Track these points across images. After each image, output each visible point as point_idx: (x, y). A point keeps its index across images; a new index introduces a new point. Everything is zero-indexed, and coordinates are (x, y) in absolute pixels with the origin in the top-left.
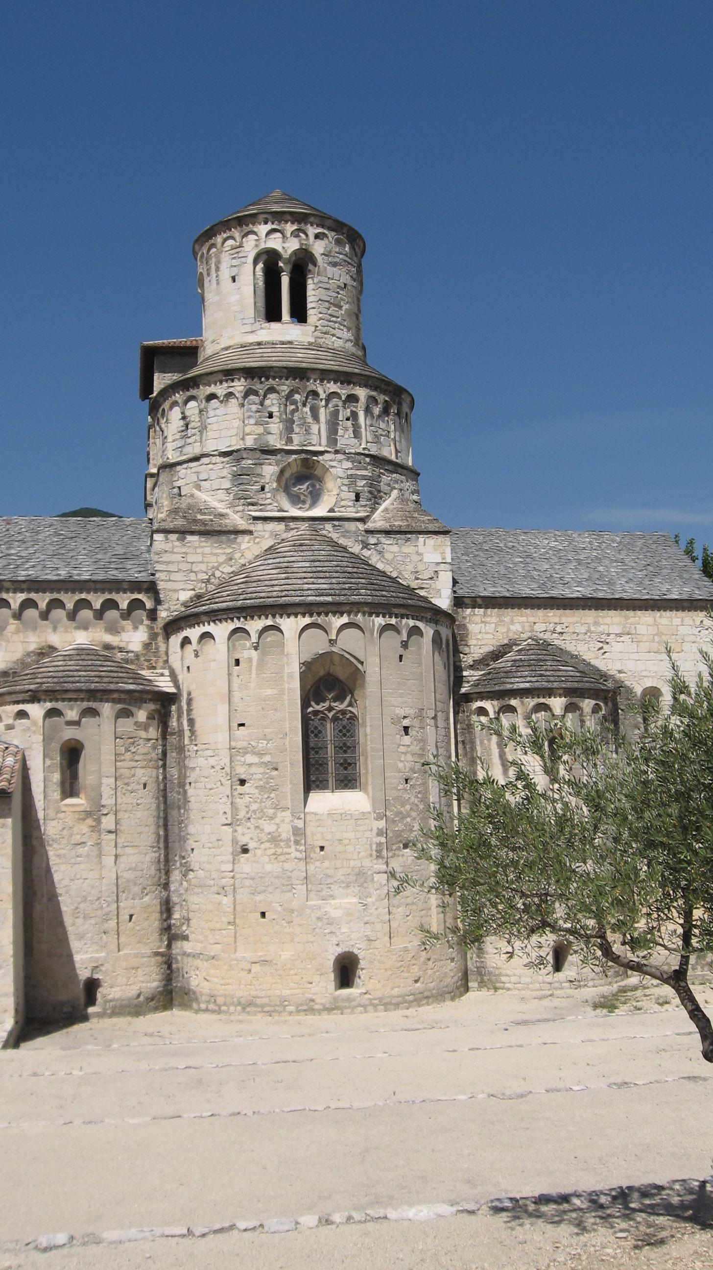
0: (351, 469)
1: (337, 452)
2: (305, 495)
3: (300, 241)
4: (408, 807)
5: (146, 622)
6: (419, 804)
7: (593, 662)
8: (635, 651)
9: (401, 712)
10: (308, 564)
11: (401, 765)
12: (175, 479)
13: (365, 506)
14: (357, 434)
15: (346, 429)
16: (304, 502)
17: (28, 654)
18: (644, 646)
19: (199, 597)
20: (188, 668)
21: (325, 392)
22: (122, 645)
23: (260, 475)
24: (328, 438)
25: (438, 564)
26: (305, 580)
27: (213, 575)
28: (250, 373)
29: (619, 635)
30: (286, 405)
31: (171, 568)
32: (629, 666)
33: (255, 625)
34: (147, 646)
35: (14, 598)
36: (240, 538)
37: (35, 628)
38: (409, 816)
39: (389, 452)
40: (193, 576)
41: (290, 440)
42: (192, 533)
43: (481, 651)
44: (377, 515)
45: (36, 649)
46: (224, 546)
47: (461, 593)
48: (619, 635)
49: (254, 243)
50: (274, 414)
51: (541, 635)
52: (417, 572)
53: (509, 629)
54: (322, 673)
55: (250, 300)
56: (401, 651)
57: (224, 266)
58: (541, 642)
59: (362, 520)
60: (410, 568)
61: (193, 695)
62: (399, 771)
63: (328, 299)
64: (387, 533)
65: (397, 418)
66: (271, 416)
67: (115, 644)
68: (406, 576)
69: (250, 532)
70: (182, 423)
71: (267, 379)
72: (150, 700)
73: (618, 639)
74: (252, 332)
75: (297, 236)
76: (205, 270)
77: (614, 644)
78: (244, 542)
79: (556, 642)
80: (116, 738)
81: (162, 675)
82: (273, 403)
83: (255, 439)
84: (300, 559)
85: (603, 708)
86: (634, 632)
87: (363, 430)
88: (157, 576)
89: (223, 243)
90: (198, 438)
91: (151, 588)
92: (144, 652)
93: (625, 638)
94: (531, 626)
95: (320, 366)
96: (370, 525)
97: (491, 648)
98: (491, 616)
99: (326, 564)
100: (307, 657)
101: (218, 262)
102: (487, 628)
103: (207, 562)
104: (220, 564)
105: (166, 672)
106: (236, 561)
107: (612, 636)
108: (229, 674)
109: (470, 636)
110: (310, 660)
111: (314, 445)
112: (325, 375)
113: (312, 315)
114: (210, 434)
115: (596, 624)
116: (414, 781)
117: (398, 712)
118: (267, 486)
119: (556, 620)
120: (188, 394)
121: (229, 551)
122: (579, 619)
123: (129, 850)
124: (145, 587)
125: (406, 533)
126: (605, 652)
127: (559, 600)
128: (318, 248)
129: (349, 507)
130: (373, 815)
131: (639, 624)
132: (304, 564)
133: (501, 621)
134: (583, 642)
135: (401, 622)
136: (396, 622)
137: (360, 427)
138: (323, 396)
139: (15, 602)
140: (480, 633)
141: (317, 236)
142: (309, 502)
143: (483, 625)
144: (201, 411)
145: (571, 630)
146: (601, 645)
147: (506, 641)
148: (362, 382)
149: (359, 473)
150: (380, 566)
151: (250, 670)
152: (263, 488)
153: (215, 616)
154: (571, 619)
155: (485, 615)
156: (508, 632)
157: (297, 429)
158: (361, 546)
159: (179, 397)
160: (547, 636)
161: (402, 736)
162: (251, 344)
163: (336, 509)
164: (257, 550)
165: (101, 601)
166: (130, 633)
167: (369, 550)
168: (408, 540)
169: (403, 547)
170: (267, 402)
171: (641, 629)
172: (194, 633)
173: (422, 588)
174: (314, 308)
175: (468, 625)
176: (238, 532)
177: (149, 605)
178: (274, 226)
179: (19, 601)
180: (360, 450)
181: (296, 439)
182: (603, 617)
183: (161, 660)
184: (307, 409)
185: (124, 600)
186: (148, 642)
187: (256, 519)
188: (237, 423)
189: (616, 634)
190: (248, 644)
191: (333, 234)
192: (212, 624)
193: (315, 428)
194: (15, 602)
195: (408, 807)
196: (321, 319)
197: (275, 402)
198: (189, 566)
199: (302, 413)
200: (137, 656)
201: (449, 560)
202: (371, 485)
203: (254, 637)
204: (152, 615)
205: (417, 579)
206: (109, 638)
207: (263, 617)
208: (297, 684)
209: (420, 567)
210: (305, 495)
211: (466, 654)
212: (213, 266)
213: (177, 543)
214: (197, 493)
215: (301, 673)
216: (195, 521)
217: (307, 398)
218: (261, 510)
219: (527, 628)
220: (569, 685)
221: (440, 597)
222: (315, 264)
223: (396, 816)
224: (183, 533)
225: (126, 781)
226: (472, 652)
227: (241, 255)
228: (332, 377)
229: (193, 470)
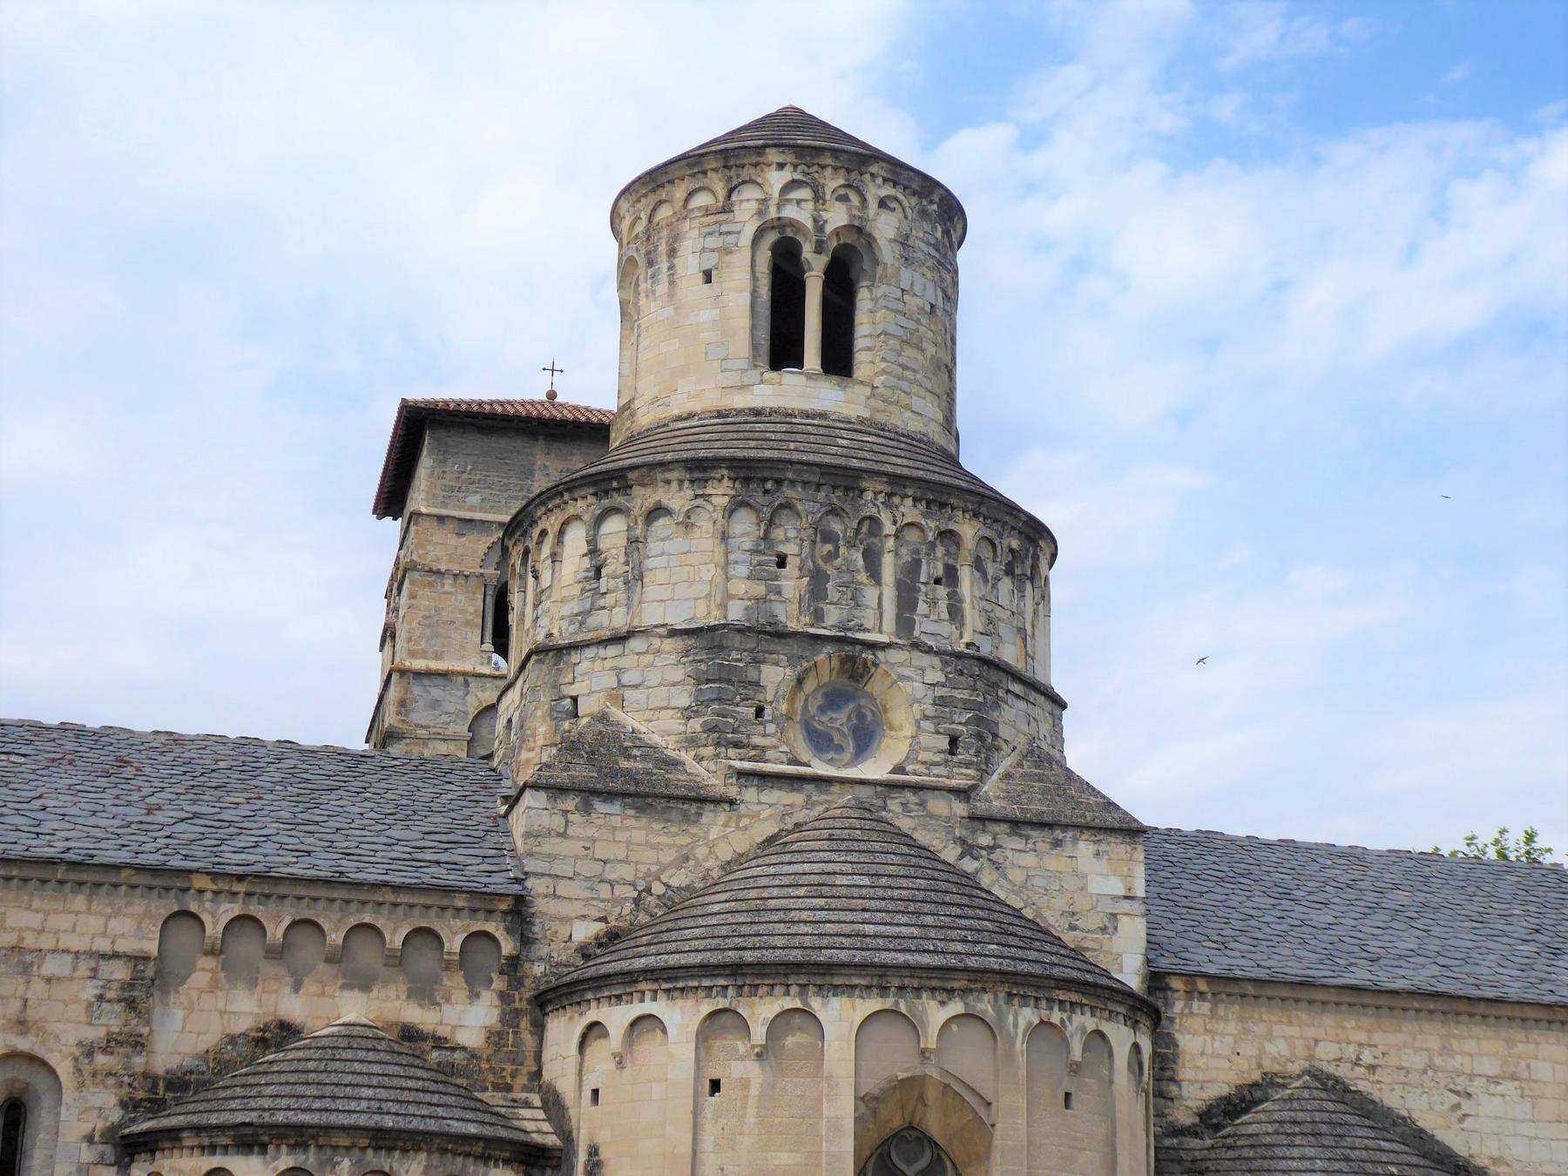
0: (943, 685)
1: (916, 645)
2: (843, 734)
3: (849, 209)
5: (499, 983)
7: (1440, 1135)
10: (866, 881)
12: (566, 680)
13: (968, 765)
14: (955, 613)
15: (933, 603)
16: (840, 749)
17: (233, 1040)
19: (613, 936)
20: (596, 1092)
21: (895, 523)
22: (443, 1031)
23: (756, 684)
24: (899, 618)
25: (1115, 898)
26: (867, 915)
27: (648, 890)
28: (747, 472)
29: (1495, 1080)
30: (814, 542)
31: (557, 869)
33: (762, 1011)
34: (496, 1038)
35: (213, 915)
36: (708, 815)
37: (252, 983)
39: (1009, 654)
40: (604, 890)
41: (818, 616)
42: (610, 796)
43: (1205, 1096)
44: (991, 786)
45: (251, 1030)
46: (674, 829)
47: (1164, 963)
48: (1495, 1080)
49: (754, 206)
50: (789, 559)
51: (1331, 1069)
52: (1073, 914)
53: (1262, 1050)
54: (897, 1122)
55: (742, 322)
56: (1068, 1084)
57: (688, 246)
58: (1330, 1083)
59: (963, 794)
60: (1060, 903)
61: (604, 1154)
63: (900, 332)
64: (1016, 825)
66: (781, 562)
67: (427, 1028)
69: (732, 802)
70: (586, 562)
71: (779, 482)
72: (506, 1162)
73: (1493, 1088)
74: (743, 387)
75: (844, 199)
76: (643, 251)
77: (1483, 1098)
78: (714, 823)
79: (1363, 1086)
81: (527, 1105)
82: (790, 538)
83: (747, 609)
84: (848, 868)
86: (1525, 1075)
88: (529, 884)
89: (687, 200)
90: (622, 596)
91: (519, 912)
92: (490, 1051)
93: (1508, 1087)
94: (1308, 1048)
95: (889, 469)
96: (981, 807)
97: (1224, 1090)
98: (1226, 1019)
99: (904, 883)
100: (871, 1085)
101: (676, 238)
102: (1217, 1044)
103: (637, 863)
104: (664, 868)
105: (536, 1099)
106: (698, 863)
107: (1478, 1082)
108: (696, 1113)
109: (1180, 1061)
110: (876, 1092)
111: (868, 630)
112: (898, 482)
113: (865, 361)
114: (651, 592)
115: (1446, 1051)
118: (768, 711)
119: (1362, 1037)
120: (606, 502)
121: (683, 840)
124: (503, 906)
125: (1049, 826)
126: (1465, 1115)
128: (885, 227)
131: (1536, 1058)
132: (857, 880)
133: (1247, 1032)
134: (1419, 1091)
135: (1070, 1019)
136: (1062, 1021)
137: (961, 601)
139: (215, 923)
140: (1202, 1054)
141: (882, 204)
142: (850, 747)
143: (1209, 1039)
144: (633, 541)
145: (1392, 1060)
146: (1455, 1099)
147: (1256, 1076)
149: (957, 694)
151: (744, 1107)
152: (759, 712)
153: (670, 979)
154: (1393, 1038)
155: (1213, 1015)
158: (960, 850)
159: (585, 506)
160: (1343, 1071)
162: (739, 412)
163: (909, 768)
164: (741, 843)
165: (405, 931)
166: (459, 1008)
167: (976, 859)
168: (1057, 844)
169: (1046, 858)
170: (778, 534)
171: (1542, 1071)
172: (617, 1017)
174: (869, 349)
175: (1177, 1036)
176: (702, 800)
177: (508, 946)
178: (798, 176)
179: (224, 920)
180: (961, 648)
181: (833, 615)
182: (1460, 1038)
183: (524, 1070)
185: (455, 933)
186: (499, 1027)
187: (741, 774)
188: (709, 572)
189: (1488, 1077)
190: (742, 1047)
191: (914, 200)
192: (661, 996)
193: (870, 594)
194: (215, 923)
196: (884, 372)
197: (792, 534)
198: (598, 867)
199: (848, 561)
200: (473, 1055)
201: (1140, 892)
202: (978, 721)
203: (759, 1034)
204: (513, 966)
205: (1073, 928)
206: (415, 1015)
207: (778, 990)
208: (847, 1145)
209: (1081, 904)
210: (843, 734)
211: (1172, 1099)
212: (663, 248)
214: (616, 713)
215: (856, 1119)
216: (616, 773)
217: (857, 531)
218: (750, 759)
219: (1301, 1051)
222: (876, 262)
224: (589, 794)
226: (1185, 1094)
227: (724, 228)
228: (910, 492)
229: (608, 664)
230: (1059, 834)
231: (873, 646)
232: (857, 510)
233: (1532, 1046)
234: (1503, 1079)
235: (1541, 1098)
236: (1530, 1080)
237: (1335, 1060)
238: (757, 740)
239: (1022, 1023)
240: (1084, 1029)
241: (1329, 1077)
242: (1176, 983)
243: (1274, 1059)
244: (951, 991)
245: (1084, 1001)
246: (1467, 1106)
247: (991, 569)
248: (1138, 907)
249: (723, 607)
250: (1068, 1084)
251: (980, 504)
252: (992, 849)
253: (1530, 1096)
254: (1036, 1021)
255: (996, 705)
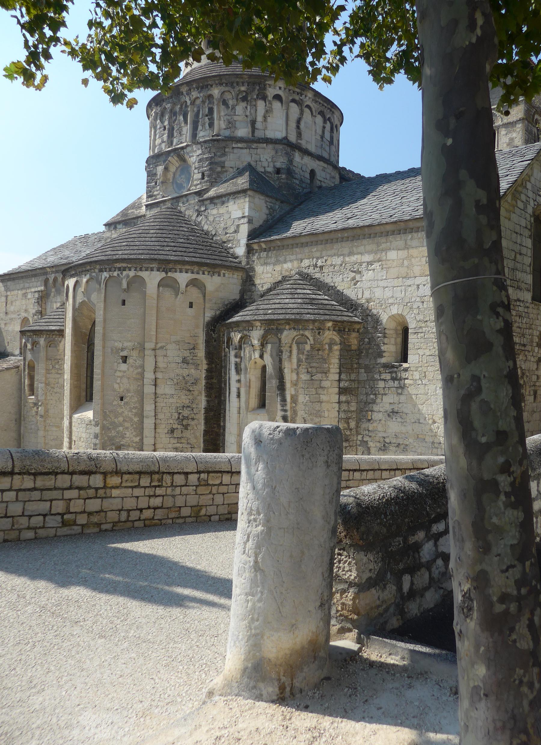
4: (121, 419)
6: (133, 417)
8: (384, 277)
9: (119, 345)
11: (116, 386)
14: (211, 125)
15: (203, 125)
18: (394, 272)
23: (156, 174)
25: (240, 219)
29: (370, 263)
32: (378, 293)
38: (121, 425)
39: (243, 132)
41: (171, 143)
48: (370, 263)
51: (306, 271)
53: (282, 268)
60: (222, 225)
62: (114, 390)
65: (261, 104)
68: (220, 233)
77: (364, 273)
79: (317, 276)
80: (47, 359)
85: (311, 338)
87: (216, 122)
98: (271, 257)
107: (364, 265)
109: (256, 277)
115: (351, 254)
116: (128, 398)
117: (116, 344)
118: (158, 181)
119: (318, 254)
122: (336, 251)
123: (54, 429)
126: (358, 281)
127: (320, 236)
129: (198, 185)
130: (93, 423)
134: (339, 273)
135: (122, 273)
136: (118, 274)
138: (189, 102)
147: (280, 278)
148: (217, 82)
150: (206, 228)
155: (267, 256)
156: (281, 271)
157: (175, 134)
160: (311, 271)
161: (119, 363)
173: (230, 241)
181: (175, 141)
182: (357, 247)
184: (181, 118)
195: (121, 419)
209: (229, 223)
213: (113, 232)
218: (154, 199)
220: (267, 317)
221: (239, 246)
223: (111, 425)
225: (52, 385)
228: (194, 86)
230: (224, 199)
231: (182, 148)
232: (179, 101)
233: (388, 244)
234: (375, 262)
235: (390, 267)
236: (386, 260)
237: (307, 266)
238: (155, 193)
239: (103, 277)
240: (128, 276)
241: (306, 274)
242: (255, 247)
243: (286, 270)
244: (88, 271)
245: (129, 266)
246: (358, 277)
247: (231, 103)
248: (246, 220)
249: (154, 151)
250: (123, 296)
251: (221, 80)
252: (205, 210)
253: (385, 268)
254: (108, 276)
255: (224, 154)
